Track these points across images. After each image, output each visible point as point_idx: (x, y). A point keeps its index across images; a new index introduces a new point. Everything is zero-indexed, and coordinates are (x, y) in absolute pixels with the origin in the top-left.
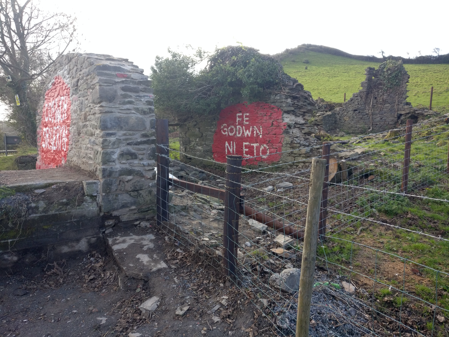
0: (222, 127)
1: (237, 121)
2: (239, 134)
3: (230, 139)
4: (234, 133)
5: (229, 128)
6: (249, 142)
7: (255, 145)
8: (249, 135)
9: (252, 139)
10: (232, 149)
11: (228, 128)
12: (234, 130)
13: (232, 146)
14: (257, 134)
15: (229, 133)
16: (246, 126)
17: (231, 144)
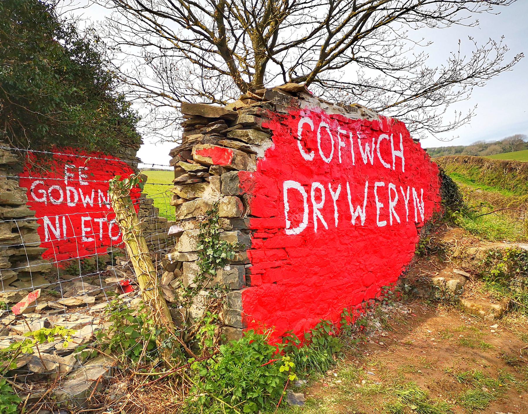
2: (72, 200)
4: (61, 200)
7: (101, 221)
8: (91, 202)
10: (58, 230)
12: (61, 192)
13: (58, 225)
16: (83, 187)
17: (57, 221)
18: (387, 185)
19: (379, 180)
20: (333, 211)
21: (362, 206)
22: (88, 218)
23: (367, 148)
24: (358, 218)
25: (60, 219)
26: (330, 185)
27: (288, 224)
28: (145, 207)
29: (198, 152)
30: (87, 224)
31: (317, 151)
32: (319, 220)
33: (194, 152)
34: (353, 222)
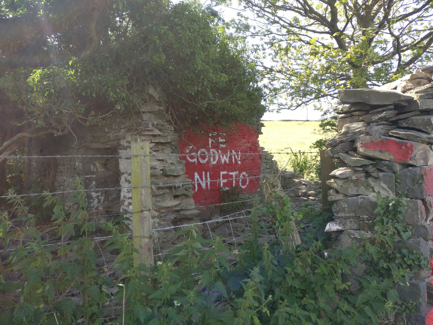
1: (210, 143)
2: (214, 160)
3: (201, 168)
4: (207, 159)
6: (228, 171)
7: (234, 174)
8: (227, 161)
9: (230, 166)
10: (204, 183)
12: (206, 153)
13: (204, 179)
14: (235, 159)
15: (201, 161)
16: (222, 149)
17: (204, 176)
22: (225, 173)
28: (266, 161)
29: (364, 145)
30: (224, 177)
33: (358, 145)
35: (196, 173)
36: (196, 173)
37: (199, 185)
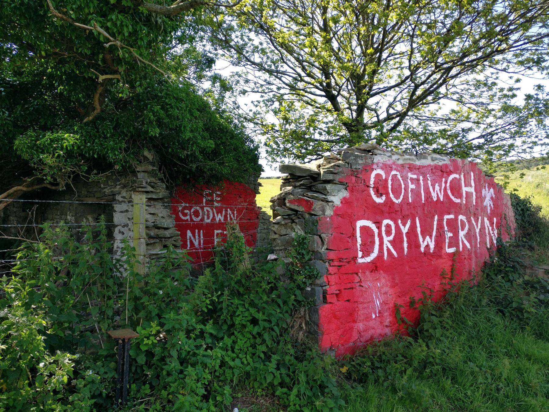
0: (180, 209)
2: (208, 218)
3: (194, 227)
4: (200, 218)
5: (192, 210)
10: (197, 240)
11: (190, 211)
12: (200, 211)
13: (197, 237)
15: (194, 219)
16: (216, 208)
17: (197, 234)
18: (456, 219)
19: (449, 214)
20: (403, 241)
21: (431, 237)
22: (220, 231)
23: (437, 187)
24: (427, 246)
25: (199, 233)
26: (400, 221)
27: (360, 254)
28: (263, 221)
29: (290, 202)
31: (387, 194)
32: (388, 250)
33: (287, 201)
34: (422, 249)
35: (188, 231)
36: (188, 231)
37: (191, 242)
